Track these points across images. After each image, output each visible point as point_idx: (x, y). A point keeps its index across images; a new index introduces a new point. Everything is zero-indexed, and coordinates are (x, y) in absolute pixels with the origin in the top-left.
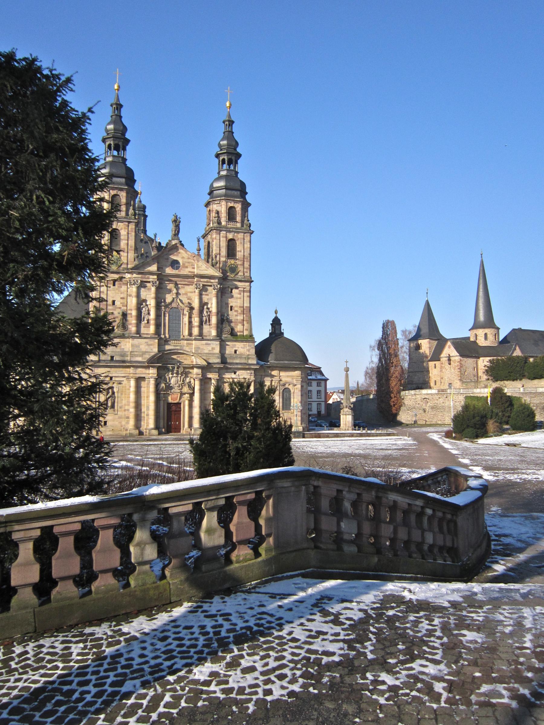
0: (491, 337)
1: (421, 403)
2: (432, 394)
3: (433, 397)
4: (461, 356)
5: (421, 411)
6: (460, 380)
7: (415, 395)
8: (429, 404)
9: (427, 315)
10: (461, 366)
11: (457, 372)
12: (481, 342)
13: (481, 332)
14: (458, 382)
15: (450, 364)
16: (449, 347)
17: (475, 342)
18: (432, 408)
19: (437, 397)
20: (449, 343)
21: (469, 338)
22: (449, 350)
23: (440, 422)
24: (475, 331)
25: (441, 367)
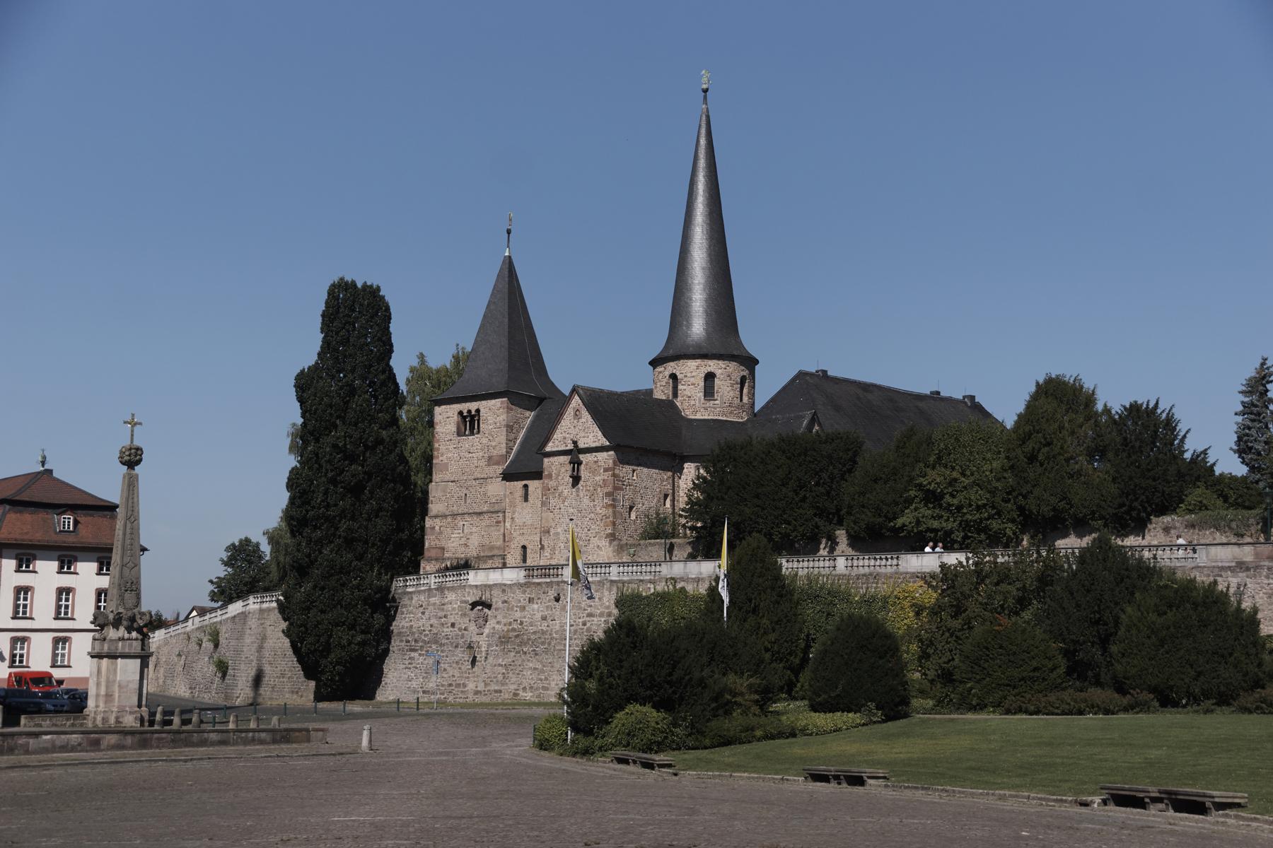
0: (725, 389)
1: (462, 622)
2: (503, 587)
3: (510, 596)
4: (614, 447)
5: (462, 655)
6: (612, 537)
7: (441, 589)
8: (492, 623)
9: (504, 307)
10: (618, 485)
11: (600, 507)
12: (693, 404)
13: (692, 372)
14: (604, 543)
15: (576, 480)
16: (577, 414)
17: (669, 407)
18: (504, 640)
19: (520, 597)
20: (576, 402)
21: (650, 392)
22: (578, 428)
23: (528, 696)
24: (671, 367)
25: (546, 489)
